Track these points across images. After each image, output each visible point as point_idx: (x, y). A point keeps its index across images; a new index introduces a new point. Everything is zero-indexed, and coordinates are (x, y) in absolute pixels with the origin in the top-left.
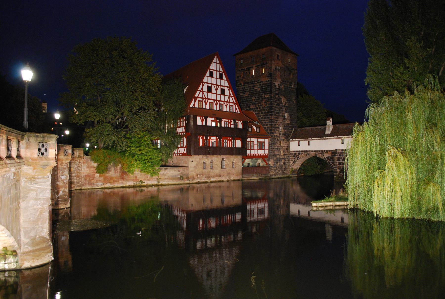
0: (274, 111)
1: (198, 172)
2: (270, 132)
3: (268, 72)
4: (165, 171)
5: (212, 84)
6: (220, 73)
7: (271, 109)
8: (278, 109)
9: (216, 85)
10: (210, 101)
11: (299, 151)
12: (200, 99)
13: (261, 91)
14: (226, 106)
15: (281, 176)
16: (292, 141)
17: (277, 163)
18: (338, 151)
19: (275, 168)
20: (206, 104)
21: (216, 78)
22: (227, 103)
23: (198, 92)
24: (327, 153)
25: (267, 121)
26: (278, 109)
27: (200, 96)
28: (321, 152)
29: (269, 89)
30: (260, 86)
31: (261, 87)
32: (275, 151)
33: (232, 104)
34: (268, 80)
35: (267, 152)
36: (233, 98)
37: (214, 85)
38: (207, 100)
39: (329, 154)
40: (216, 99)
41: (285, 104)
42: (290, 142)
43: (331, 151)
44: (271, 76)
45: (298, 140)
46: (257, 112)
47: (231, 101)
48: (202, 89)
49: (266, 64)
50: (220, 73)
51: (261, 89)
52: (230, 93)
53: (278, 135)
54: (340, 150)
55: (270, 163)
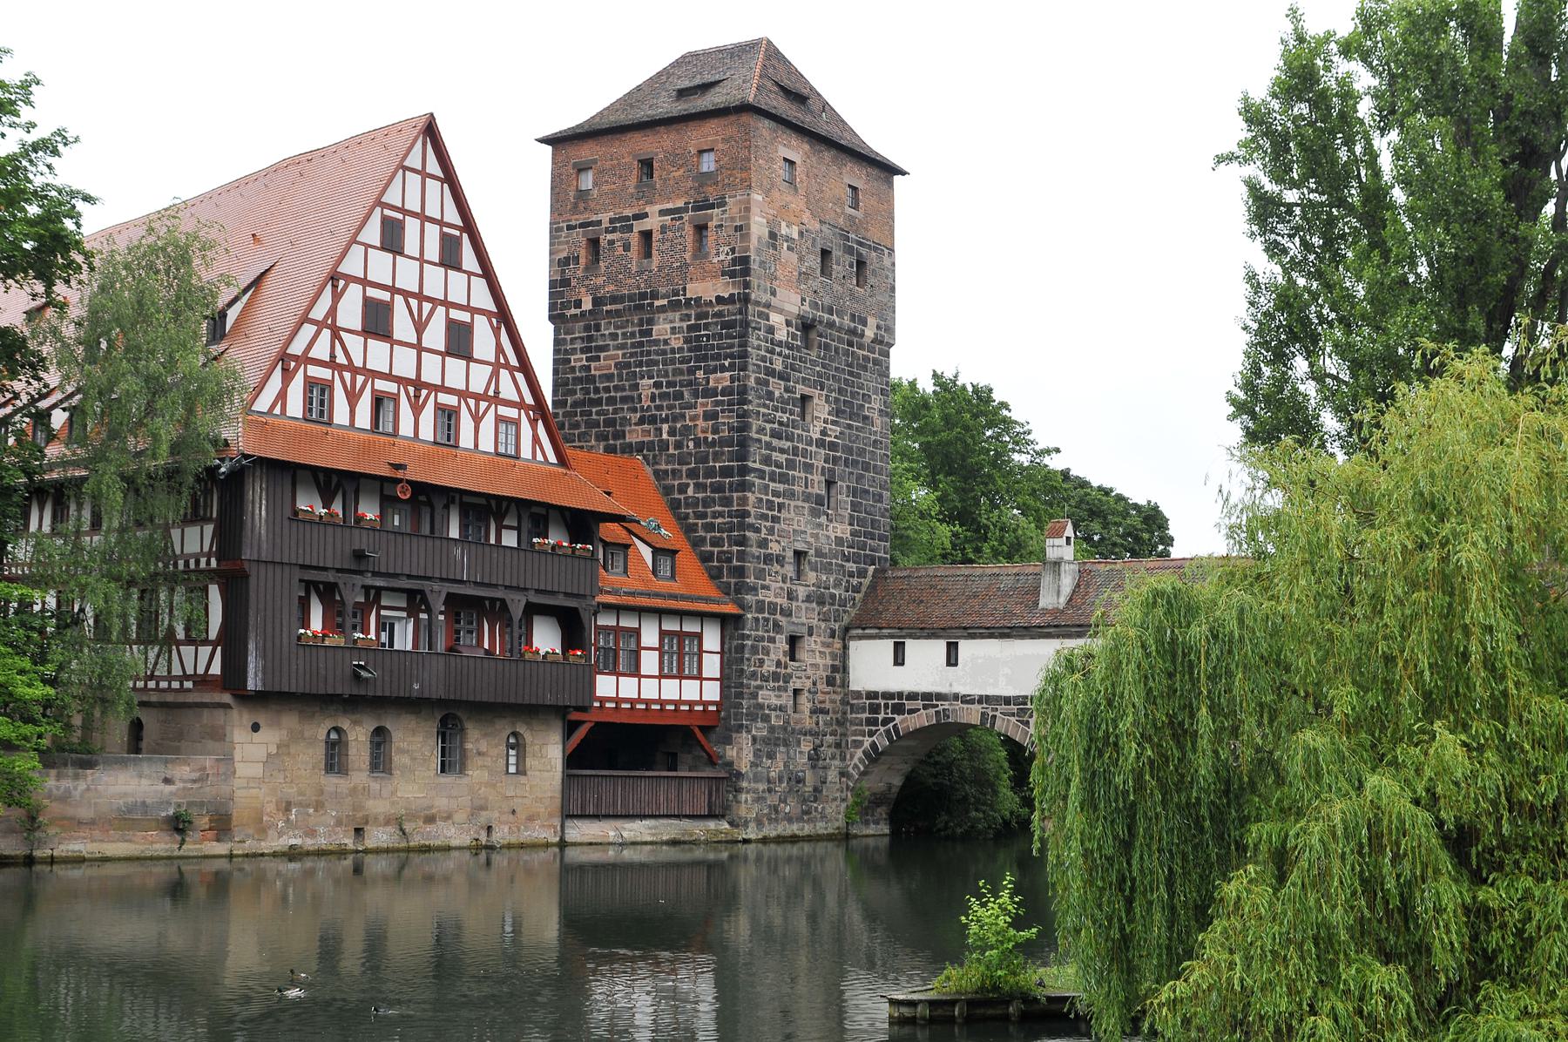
0: (757, 465)
1: (291, 792)
2: (733, 580)
3: (727, 248)
4: (76, 777)
5: (393, 290)
6: (446, 230)
7: (742, 456)
8: (782, 458)
9: (420, 297)
10: (382, 385)
11: (900, 695)
12: (315, 372)
13: (690, 350)
14: (477, 419)
15: (794, 828)
16: (860, 638)
17: (771, 756)
19: (762, 786)
20: (353, 397)
21: (422, 260)
22: (483, 405)
23: (308, 330)
25: (720, 520)
26: (782, 458)
27: (321, 350)
29: (732, 346)
30: (684, 325)
31: (690, 328)
32: (761, 687)
33: (512, 413)
34: (726, 296)
35: (712, 692)
36: (520, 377)
37: (406, 294)
38: (360, 379)
40: (413, 377)
41: (824, 432)
42: (853, 645)
44: (746, 272)
45: (890, 636)
46: (663, 467)
47: (507, 391)
48: (333, 312)
49: (722, 204)
50: (446, 230)
51: (687, 341)
52: (499, 349)
53: (782, 601)
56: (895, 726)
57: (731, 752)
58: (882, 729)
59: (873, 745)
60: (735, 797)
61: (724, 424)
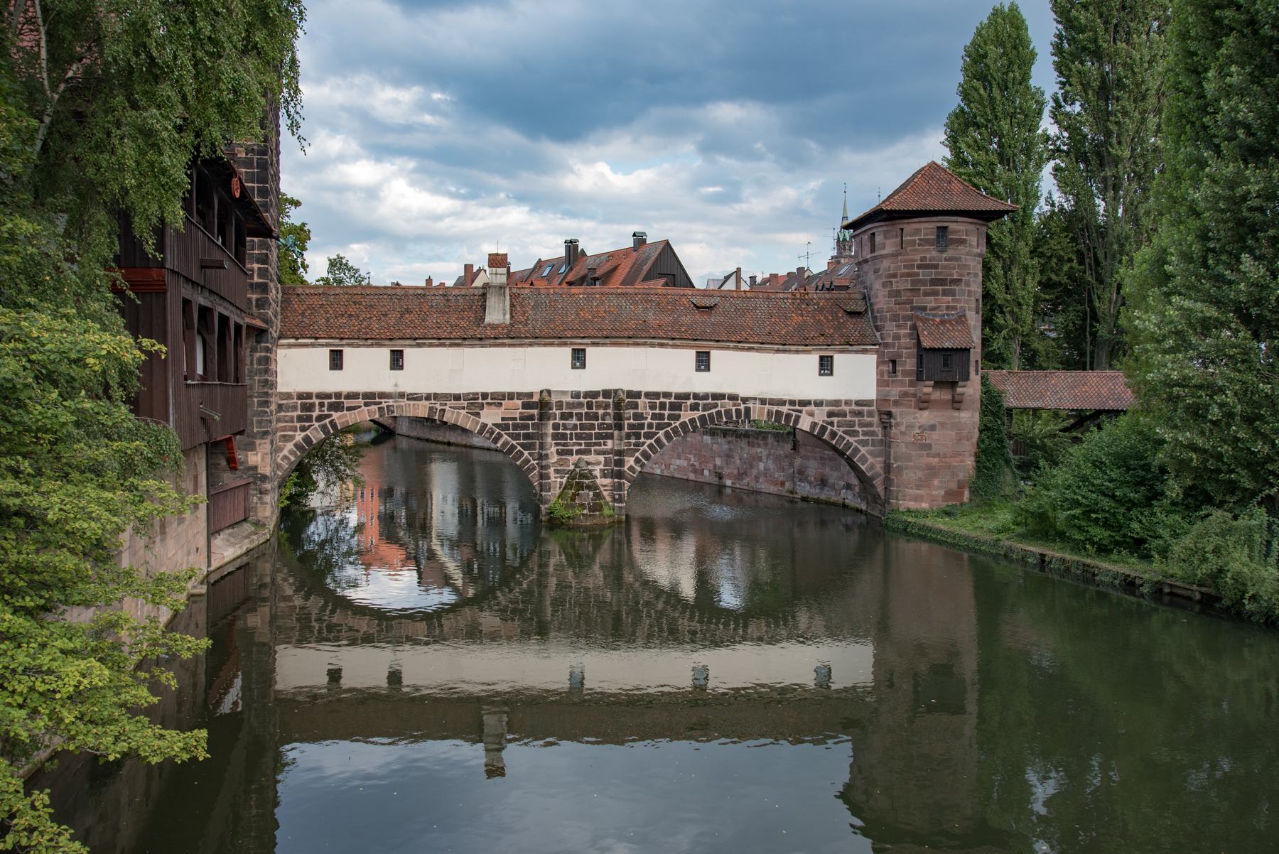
11: (338, 395)
16: (290, 346)
18: (554, 399)
24: (501, 404)
28: (465, 403)
39: (514, 409)
43: (520, 395)
45: (327, 345)
54: (564, 393)
55: (259, 458)
56: (331, 422)
57: (254, 458)
58: (316, 424)
59: (307, 440)
60: (260, 499)
61: (240, 145)
